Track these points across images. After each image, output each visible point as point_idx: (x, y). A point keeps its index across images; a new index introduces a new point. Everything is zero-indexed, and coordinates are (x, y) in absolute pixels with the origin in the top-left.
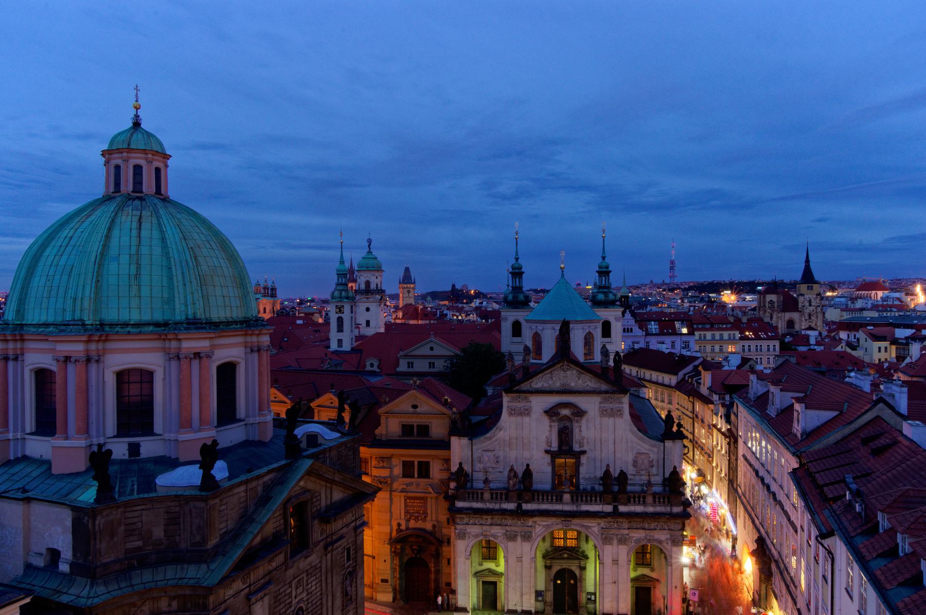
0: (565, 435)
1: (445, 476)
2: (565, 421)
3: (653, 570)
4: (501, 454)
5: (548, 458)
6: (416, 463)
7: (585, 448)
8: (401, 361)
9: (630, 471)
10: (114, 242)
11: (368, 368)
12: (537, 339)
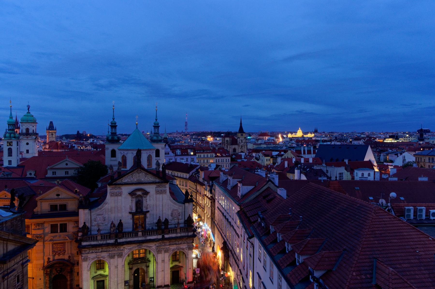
1: (76, 230)
2: (139, 197)
3: (180, 262)
4: (106, 216)
5: (131, 216)
6: (59, 225)
7: (149, 210)
8: (49, 171)
9: (170, 218)
11: (28, 176)
12: (124, 159)
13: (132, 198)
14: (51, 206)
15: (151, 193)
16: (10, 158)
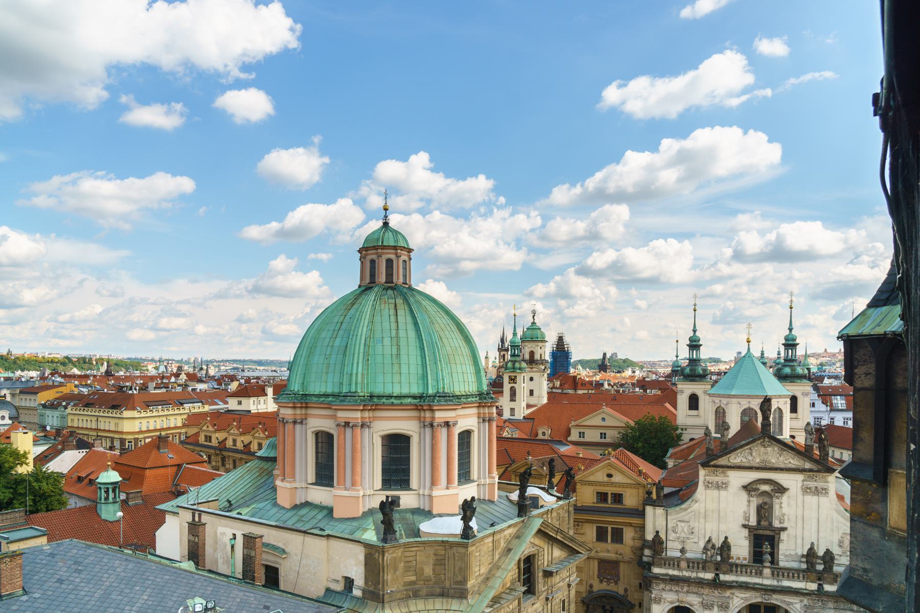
0: (764, 511)
1: (638, 544)
2: (766, 496)
4: (696, 524)
5: (745, 532)
8: (573, 431)
9: (836, 550)
10: (378, 327)
11: (540, 436)
12: (720, 414)
13: (750, 495)
16: (513, 405)
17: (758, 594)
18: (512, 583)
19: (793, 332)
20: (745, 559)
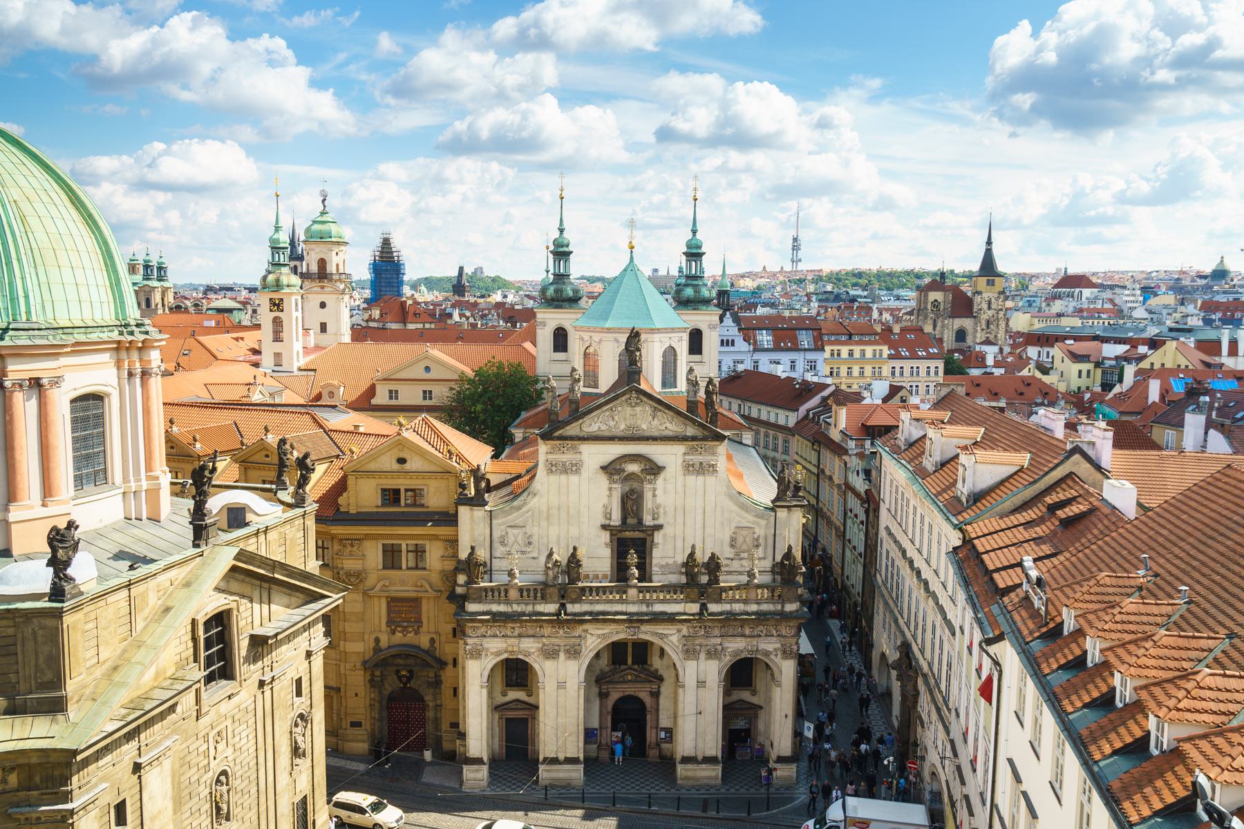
0: (631, 503)
1: (450, 565)
2: (632, 480)
4: (534, 530)
5: (606, 536)
6: (404, 548)
8: (378, 388)
9: (725, 553)
13: (612, 481)
14: (383, 490)
15: (667, 470)
16: (278, 347)
17: (622, 627)
18: (180, 666)
19: (698, 236)
20: (605, 576)
